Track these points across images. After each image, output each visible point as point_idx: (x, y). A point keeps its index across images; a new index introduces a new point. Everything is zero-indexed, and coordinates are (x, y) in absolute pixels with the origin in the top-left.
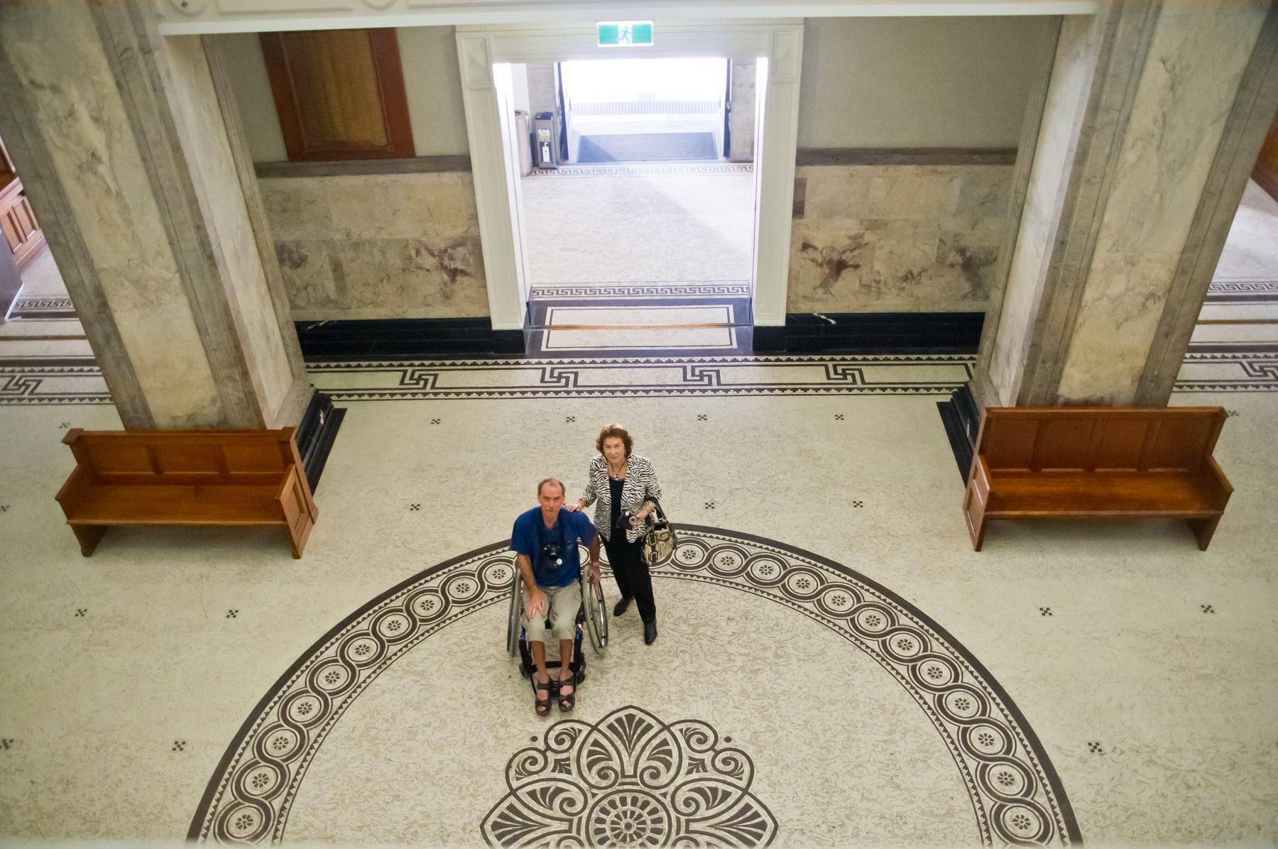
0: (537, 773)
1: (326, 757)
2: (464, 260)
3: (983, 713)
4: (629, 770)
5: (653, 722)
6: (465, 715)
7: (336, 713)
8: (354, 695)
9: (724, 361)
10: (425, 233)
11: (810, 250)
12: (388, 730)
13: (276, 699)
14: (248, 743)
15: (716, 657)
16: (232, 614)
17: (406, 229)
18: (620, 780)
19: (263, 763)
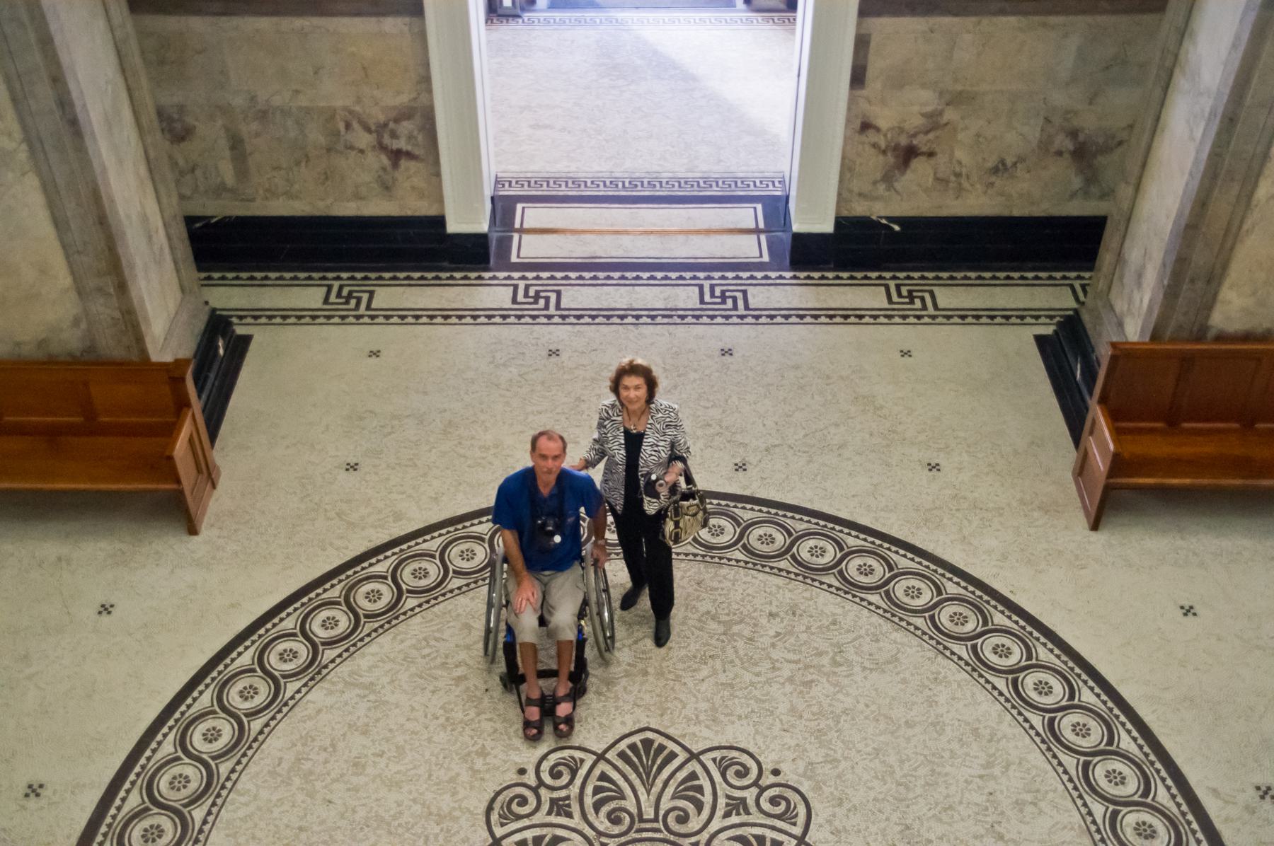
0: (528, 816)
1: (242, 799)
2: (410, 137)
3: (1110, 743)
5: (677, 749)
6: (429, 740)
7: (255, 740)
8: (279, 716)
9: (766, 277)
10: (359, 100)
11: (871, 133)
12: (326, 762)
13: (171, 722)
14: (133, 783)
15: (756, 664)
16: (106, 609)
17: (334, 94)
18: (637, 826)
19: (156, 810)
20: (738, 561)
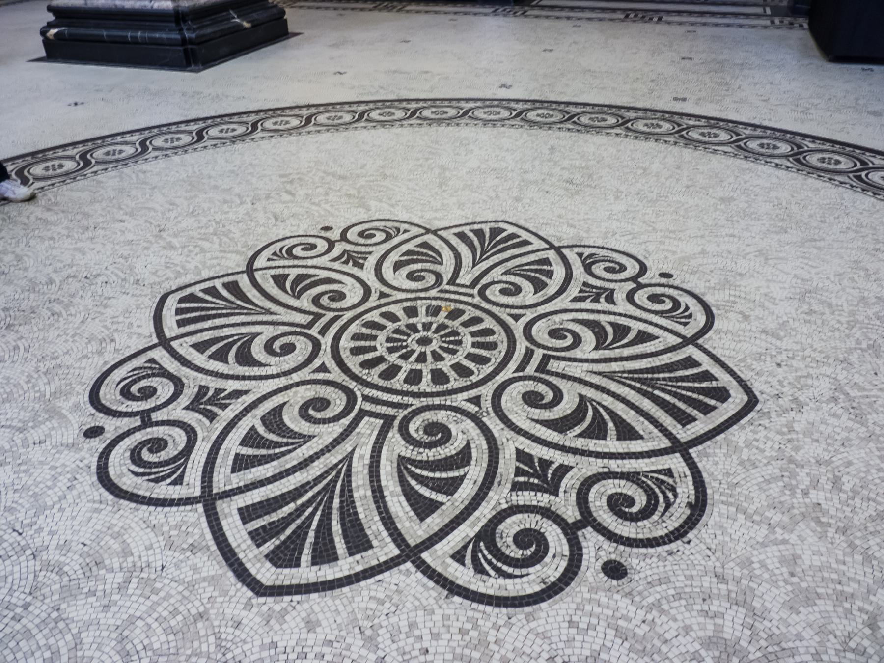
4: (369, 428)
18: (402, 414)
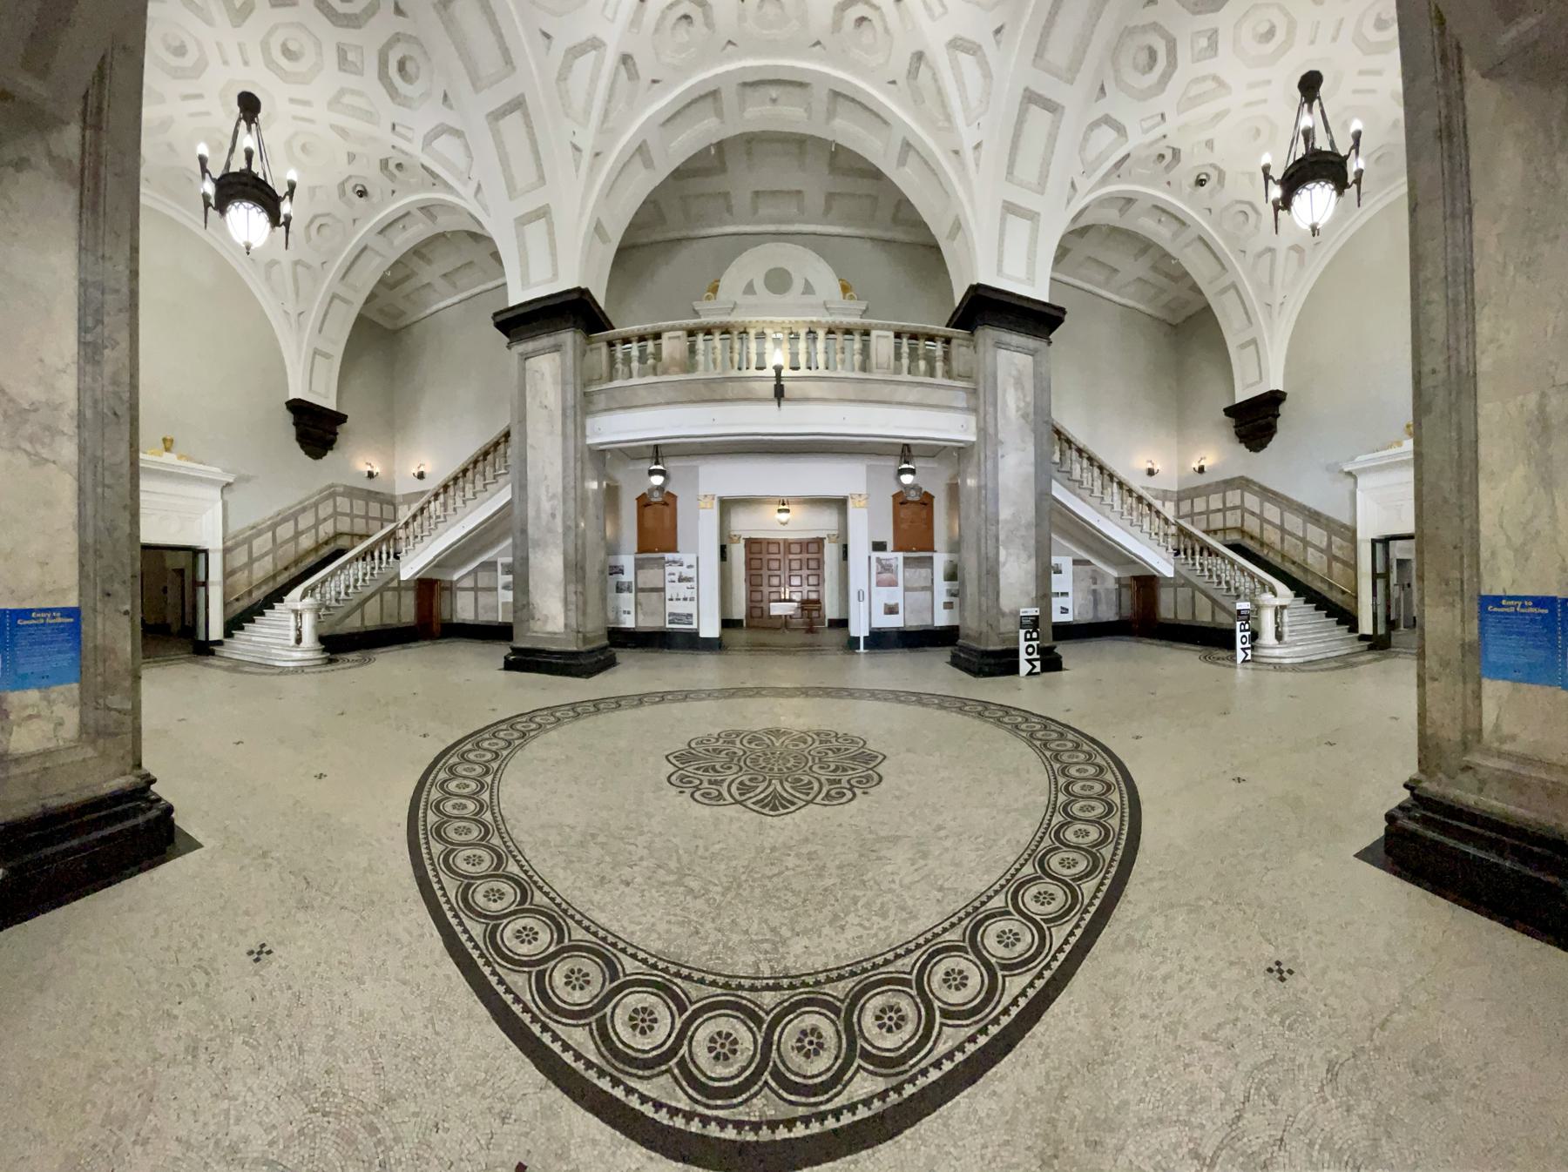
20: (634, 956)
